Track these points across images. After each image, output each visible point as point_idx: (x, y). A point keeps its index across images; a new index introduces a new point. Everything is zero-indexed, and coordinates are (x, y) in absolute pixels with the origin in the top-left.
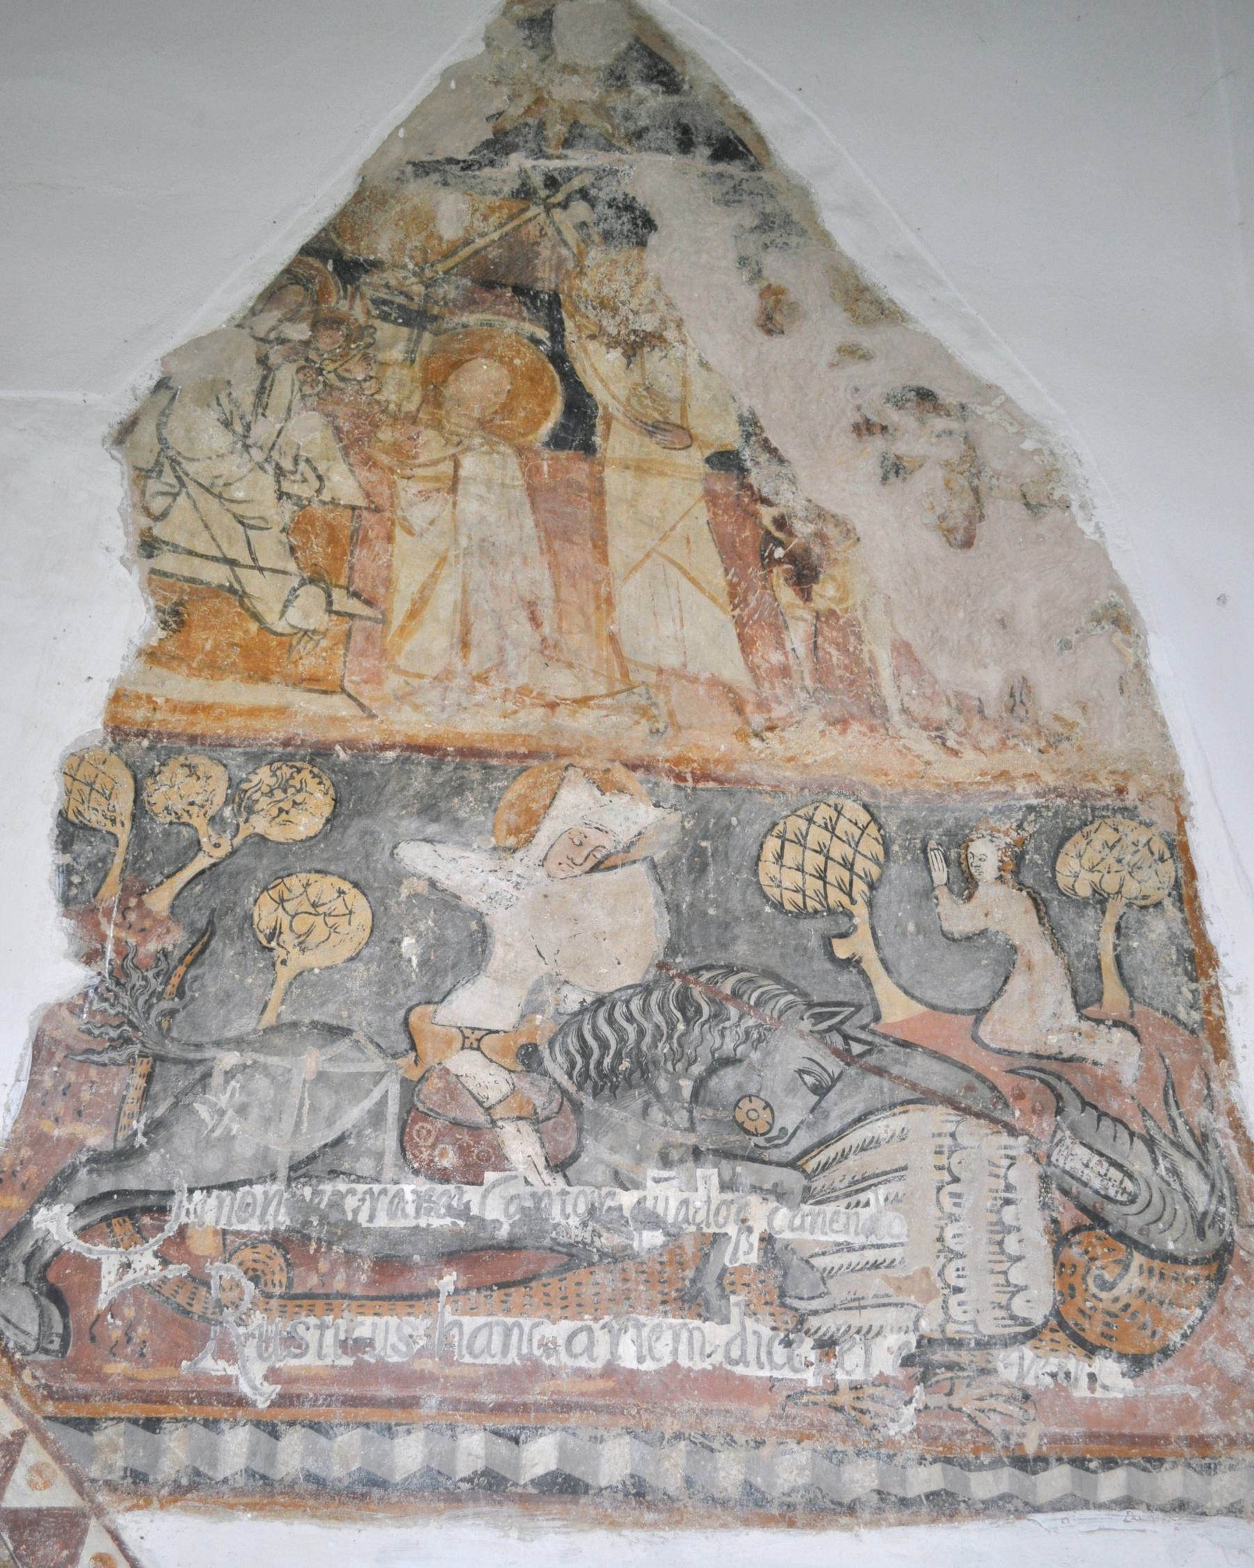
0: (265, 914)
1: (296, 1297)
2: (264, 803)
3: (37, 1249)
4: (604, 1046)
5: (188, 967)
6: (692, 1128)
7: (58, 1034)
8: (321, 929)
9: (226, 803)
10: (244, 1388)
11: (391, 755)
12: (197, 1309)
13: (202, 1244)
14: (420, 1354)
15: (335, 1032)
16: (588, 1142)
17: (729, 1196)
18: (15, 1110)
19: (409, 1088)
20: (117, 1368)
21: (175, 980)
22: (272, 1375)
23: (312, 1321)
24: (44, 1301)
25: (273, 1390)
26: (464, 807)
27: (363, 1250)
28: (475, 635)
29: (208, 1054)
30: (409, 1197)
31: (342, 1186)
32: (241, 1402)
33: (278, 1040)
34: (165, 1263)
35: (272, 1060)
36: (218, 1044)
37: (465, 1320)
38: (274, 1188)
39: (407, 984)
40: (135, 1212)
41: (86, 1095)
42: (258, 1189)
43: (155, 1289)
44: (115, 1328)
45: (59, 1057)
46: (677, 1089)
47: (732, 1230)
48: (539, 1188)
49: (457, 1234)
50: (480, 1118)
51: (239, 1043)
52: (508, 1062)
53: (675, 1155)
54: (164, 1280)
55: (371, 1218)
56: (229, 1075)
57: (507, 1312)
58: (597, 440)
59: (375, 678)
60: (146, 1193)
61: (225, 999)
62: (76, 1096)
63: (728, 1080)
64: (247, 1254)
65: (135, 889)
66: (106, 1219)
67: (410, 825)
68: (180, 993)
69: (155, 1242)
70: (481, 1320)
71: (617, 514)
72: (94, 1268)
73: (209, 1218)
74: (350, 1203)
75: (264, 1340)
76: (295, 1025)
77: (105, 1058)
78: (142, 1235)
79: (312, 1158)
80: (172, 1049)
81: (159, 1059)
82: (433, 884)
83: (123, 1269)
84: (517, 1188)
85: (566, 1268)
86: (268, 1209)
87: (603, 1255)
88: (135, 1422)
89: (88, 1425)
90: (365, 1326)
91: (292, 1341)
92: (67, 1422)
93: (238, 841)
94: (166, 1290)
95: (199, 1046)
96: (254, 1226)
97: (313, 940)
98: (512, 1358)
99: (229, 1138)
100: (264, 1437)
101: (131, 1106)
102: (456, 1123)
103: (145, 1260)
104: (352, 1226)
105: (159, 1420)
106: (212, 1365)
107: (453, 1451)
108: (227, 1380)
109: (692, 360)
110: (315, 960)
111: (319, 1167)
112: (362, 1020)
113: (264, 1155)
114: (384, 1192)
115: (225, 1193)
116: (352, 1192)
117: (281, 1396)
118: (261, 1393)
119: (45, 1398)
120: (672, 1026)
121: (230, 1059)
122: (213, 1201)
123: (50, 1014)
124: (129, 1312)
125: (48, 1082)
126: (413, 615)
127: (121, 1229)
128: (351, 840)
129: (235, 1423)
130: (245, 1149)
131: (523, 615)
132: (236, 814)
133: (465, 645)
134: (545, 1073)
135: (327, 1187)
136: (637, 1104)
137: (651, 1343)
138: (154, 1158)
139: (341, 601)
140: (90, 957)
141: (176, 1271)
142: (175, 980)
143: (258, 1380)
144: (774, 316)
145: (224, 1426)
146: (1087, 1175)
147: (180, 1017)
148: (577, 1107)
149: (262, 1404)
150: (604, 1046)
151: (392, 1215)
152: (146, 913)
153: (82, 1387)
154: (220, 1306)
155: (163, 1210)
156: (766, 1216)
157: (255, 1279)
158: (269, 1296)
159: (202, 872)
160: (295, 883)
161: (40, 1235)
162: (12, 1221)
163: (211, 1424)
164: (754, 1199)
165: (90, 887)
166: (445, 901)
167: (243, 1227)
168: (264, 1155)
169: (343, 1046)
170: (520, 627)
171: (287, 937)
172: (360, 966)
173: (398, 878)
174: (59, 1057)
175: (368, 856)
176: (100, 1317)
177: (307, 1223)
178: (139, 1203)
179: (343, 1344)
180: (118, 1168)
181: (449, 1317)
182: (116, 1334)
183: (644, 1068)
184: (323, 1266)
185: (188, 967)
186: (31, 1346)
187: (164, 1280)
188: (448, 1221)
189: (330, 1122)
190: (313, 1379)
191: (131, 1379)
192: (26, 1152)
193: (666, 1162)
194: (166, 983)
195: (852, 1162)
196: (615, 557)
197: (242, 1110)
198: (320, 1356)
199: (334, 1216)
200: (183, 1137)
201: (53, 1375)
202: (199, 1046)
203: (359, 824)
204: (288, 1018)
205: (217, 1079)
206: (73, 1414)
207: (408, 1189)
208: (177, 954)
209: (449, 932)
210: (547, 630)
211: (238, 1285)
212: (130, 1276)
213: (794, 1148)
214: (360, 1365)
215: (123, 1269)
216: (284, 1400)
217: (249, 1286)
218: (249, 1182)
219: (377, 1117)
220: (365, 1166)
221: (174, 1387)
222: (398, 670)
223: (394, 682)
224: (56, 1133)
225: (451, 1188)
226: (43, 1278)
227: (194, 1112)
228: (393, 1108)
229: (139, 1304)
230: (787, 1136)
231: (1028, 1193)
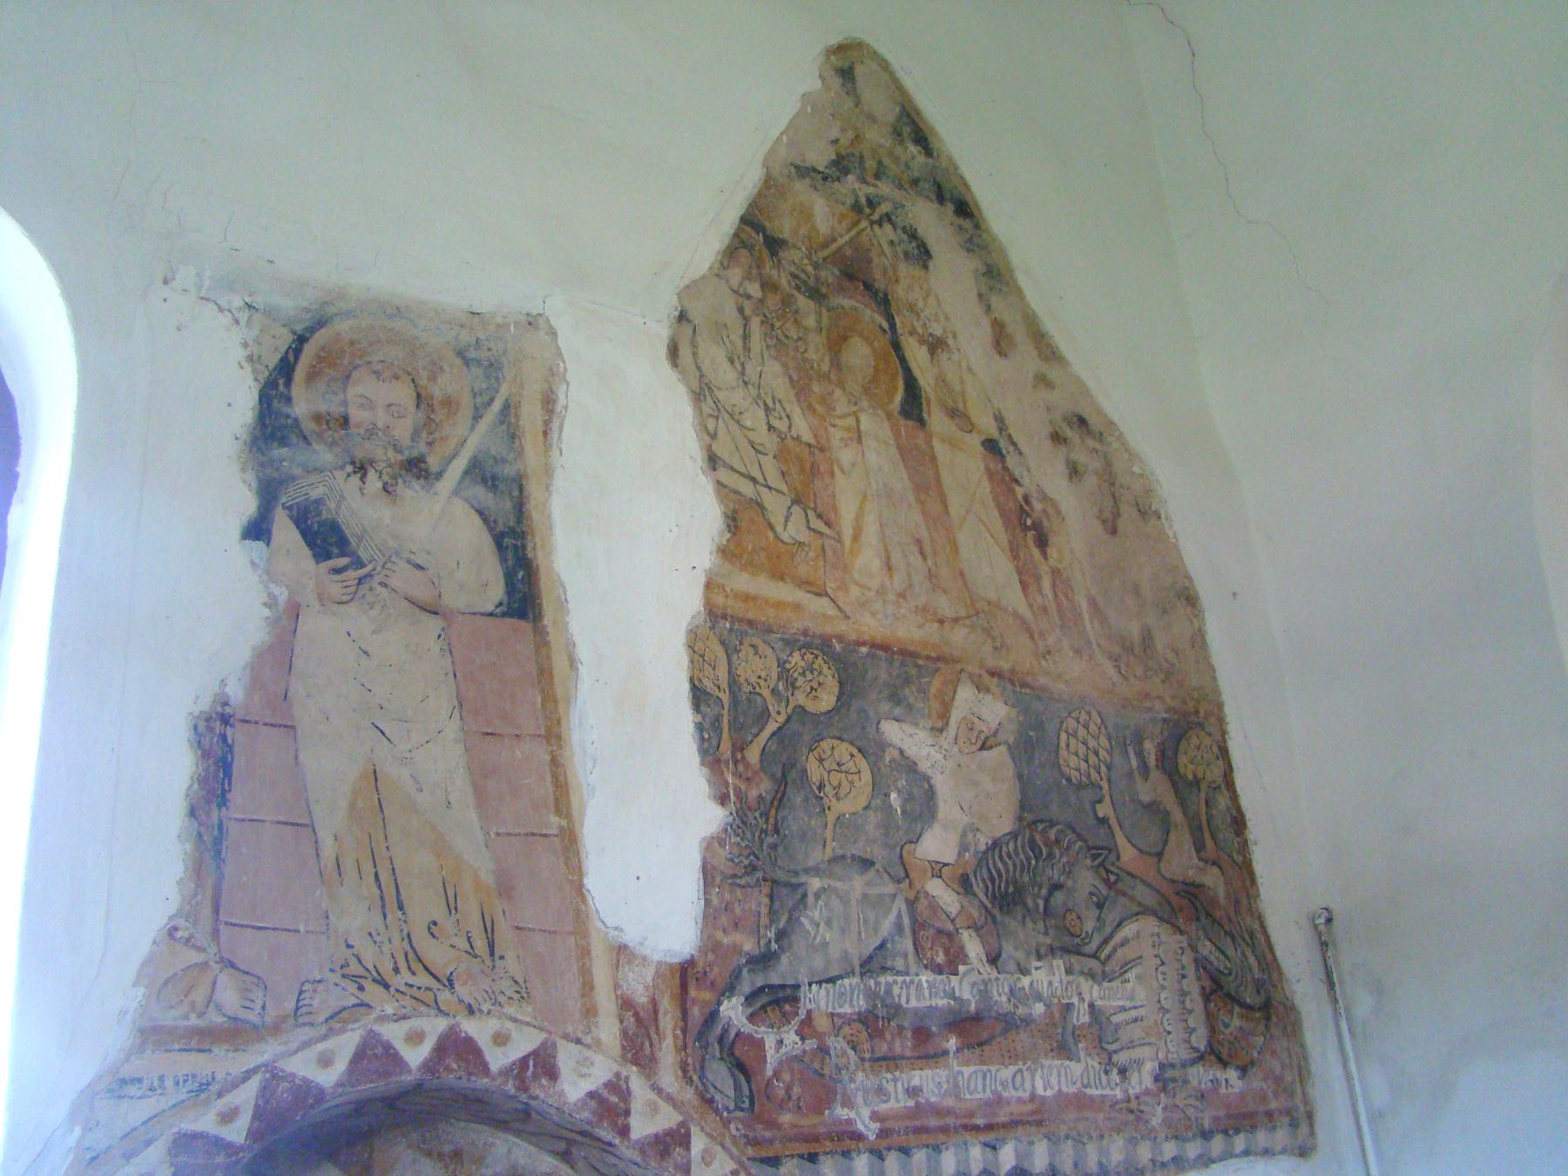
0: (815, 771)
1: (878, 1059)
2: (801, 680)
3: (725, 1031)
4: (998, 871)
5: (777, 809)
6: (1046, 934)
7: (715, 862)
8: (844, 782)
9: (779, 679)
10: (860, 1127)
11: (864, 650)
12: (826, 1072)
13: (822, 1024)
14: (944, 1096)
15: (866, 864)
16: (1004, 943)
17: (1071, 978)
18: (700, 921)
19: (911, 904)
20: (786, 1118)
21: (772, 820)
22: (875, 1116)
23: (889, 1076)
24: (737, 1072)
25: (875, 1126)
26: (910, 693)
27: (906, 1024)
28: (893, 561)
29: (803, 879)
30: (925, 985)
31: (890, 979)
32: (859, 1137)
33: (838, 869)
34: (803, 1039)
35: (839, 885)
36: (807, 871)
37: (964, 1069)
38: (856, 980)
39: (898, 828)
40: (776, 1001)
41: (738, 911)
42: (846, 981)
43: (798, 1059)
44: (779, 1088)
45: (718, 879)
46: (1037, 906)
47: (1075, 1000)
48: (986, 976)
49: (951, 1010)
50: (950, 927)
51: (817, 871)
52: (956, 887)
53: (1043, 951)
54: (804, 1051)
55: (908, 1001)
56: (817, 896)
57: (983, 1063)
58: (925, 415)
59: (843, 587)
60: (783, 987)
61: (802, 836)
62: (732, 911)
63: (1058, 898)
64: (846, 1030)
65: (739, 747)
66: (763, 1007)
67: (885, 707)
68: (777, 831)
69: (795, 1023)
70: (972, 1069)
71: (945, 476)
72: (760, 1045)
73: (822, 1004)
74: (896, 990)
75: (866, 1091)
76: (843, 857)
77: (742, 882)
78: (786, 1018)
79: (870, 958)
80: (781, 875)
81: (774, 882)
82: (902, 752)
83: (779, 1044)
84: (975, 977)
85: (1005, 1031)
86: (851, 998)
87: (1022, 1020)
88: (801, 1156)
89: (774, 1162)
90: (917, 1077)
91: (880, 1091)
92: (763, 1161)
93: (790, 710)
94: (806, 1059)
95: (796, 873)
96: (847, 1009)
97: (842, 792)
98: (988, 1094)
99: (825, 944)
100: (876, 1160)
101: (764, 920)
102: (940, 932)
103: (791, 1037)
104: (899, 1006)
105: (816, 1154)
106: (842, 1112)
107: (967, 1161)
108: (849, 1122)
109: (964, 365)
110: (845, 807)
111: (875, 964)
112: (878, 853)
113: (845, 957)
114: (912, 982)
115: (830, 985)
116: (895, 982)
117: (881, 1130)
118: (870, 1129)
119: (746, 1144)
120: (1029, 860)
121: (815, 883)
122: (823, 992)
123: (711, 845)
124: (787, 1077)
125: (715, 901)
126: (856, 538)
127: (773, 1014)
128: (853, 716)
129: (859, 1152)
130: (835, 952)
131: (915, 549)
132: (786, 689)
133: (889, 568)
134: (975, 895)
135: (882, 979)
136: (1019, 917)
137: (1051, 1078)
138: (784, 959)
139: (817, 524)
140: (723, 800)
141: (811, 1044)
142: (772, 820)
143: (867, 1120)
144: (1001, 341)
145: (854, 1155)
146: (1212, 958)
147: (780, 849)
148: (994, 917)
149: (872, 1137)
150: (1000, 875)
151: (918, 999)
152: (747, 766)
153: (768, 1134)
154: (839, 1069)
155: (796, 1000)
156: (1092, 991)
157: (854, 1048)
158: (863, 1060)
159: (774, 734)
160: (826, 745)
161: (724, 1021)
162: (707, 1011)
163: (846, 1154)
164: (1082, 979)
165: (714, 742)
166: (909, 766)
167: (842, 1011)
168: (845, 957)
169: (871, 874)
170: (915, 559)
171: (828, 789)
172: (871, 813)
173: (883, 746)
174: (718, 879)
175: (863, 728)
176: (769, 1081)
177: (875, 1006)
178: (781, 994)
179: (907, 1091)
180: (765, 969)
181: (956, 1068)
182: (781, 1093)
183: (1020, 891)
184: (888, 1036)
185: (777, 809)
186: (732, 1107)
187: (804, 1051)
188: (945, 1001)
189: (876, 931)
190: (896, 1118)
191: (795, 1126)
192: (711, 957)
193: (1039, 957)
194: (767, 822)
195: (1120, 952)
196: (953, 510)
197: (829, 923)
198: (898, 1101)
199: (889, 1001)
200: (798, 942)
201: (748, 1126)
202: (796, 873)
203: (856, 704)
204: (840, 852)
205: (811, 899)
206: (764, 1154)
207: (924, 979)
208: (769, 798)
209: (915, 790)
210: (930, 563)
211: (844, 1053)
212: (783, 1050)
213: (1094, 945)
214: (918, 1105)
215: (779, 1044)
216: (883, 1133)
217: (851, 1053)
218: (840, 977)
219: (899, 926)
220: (899, 964)
221: (822, 1130)
222: (856, 583)
223: (855, 592)
224: (725, 941)
225: (944, 977)
226: (732, 1054)
227: (801, 924)
228: (906, 921)
229: (792, 1071)
230: (1090, 936)
231: (1191, 971)
